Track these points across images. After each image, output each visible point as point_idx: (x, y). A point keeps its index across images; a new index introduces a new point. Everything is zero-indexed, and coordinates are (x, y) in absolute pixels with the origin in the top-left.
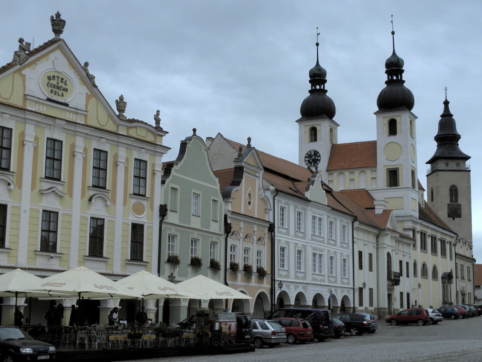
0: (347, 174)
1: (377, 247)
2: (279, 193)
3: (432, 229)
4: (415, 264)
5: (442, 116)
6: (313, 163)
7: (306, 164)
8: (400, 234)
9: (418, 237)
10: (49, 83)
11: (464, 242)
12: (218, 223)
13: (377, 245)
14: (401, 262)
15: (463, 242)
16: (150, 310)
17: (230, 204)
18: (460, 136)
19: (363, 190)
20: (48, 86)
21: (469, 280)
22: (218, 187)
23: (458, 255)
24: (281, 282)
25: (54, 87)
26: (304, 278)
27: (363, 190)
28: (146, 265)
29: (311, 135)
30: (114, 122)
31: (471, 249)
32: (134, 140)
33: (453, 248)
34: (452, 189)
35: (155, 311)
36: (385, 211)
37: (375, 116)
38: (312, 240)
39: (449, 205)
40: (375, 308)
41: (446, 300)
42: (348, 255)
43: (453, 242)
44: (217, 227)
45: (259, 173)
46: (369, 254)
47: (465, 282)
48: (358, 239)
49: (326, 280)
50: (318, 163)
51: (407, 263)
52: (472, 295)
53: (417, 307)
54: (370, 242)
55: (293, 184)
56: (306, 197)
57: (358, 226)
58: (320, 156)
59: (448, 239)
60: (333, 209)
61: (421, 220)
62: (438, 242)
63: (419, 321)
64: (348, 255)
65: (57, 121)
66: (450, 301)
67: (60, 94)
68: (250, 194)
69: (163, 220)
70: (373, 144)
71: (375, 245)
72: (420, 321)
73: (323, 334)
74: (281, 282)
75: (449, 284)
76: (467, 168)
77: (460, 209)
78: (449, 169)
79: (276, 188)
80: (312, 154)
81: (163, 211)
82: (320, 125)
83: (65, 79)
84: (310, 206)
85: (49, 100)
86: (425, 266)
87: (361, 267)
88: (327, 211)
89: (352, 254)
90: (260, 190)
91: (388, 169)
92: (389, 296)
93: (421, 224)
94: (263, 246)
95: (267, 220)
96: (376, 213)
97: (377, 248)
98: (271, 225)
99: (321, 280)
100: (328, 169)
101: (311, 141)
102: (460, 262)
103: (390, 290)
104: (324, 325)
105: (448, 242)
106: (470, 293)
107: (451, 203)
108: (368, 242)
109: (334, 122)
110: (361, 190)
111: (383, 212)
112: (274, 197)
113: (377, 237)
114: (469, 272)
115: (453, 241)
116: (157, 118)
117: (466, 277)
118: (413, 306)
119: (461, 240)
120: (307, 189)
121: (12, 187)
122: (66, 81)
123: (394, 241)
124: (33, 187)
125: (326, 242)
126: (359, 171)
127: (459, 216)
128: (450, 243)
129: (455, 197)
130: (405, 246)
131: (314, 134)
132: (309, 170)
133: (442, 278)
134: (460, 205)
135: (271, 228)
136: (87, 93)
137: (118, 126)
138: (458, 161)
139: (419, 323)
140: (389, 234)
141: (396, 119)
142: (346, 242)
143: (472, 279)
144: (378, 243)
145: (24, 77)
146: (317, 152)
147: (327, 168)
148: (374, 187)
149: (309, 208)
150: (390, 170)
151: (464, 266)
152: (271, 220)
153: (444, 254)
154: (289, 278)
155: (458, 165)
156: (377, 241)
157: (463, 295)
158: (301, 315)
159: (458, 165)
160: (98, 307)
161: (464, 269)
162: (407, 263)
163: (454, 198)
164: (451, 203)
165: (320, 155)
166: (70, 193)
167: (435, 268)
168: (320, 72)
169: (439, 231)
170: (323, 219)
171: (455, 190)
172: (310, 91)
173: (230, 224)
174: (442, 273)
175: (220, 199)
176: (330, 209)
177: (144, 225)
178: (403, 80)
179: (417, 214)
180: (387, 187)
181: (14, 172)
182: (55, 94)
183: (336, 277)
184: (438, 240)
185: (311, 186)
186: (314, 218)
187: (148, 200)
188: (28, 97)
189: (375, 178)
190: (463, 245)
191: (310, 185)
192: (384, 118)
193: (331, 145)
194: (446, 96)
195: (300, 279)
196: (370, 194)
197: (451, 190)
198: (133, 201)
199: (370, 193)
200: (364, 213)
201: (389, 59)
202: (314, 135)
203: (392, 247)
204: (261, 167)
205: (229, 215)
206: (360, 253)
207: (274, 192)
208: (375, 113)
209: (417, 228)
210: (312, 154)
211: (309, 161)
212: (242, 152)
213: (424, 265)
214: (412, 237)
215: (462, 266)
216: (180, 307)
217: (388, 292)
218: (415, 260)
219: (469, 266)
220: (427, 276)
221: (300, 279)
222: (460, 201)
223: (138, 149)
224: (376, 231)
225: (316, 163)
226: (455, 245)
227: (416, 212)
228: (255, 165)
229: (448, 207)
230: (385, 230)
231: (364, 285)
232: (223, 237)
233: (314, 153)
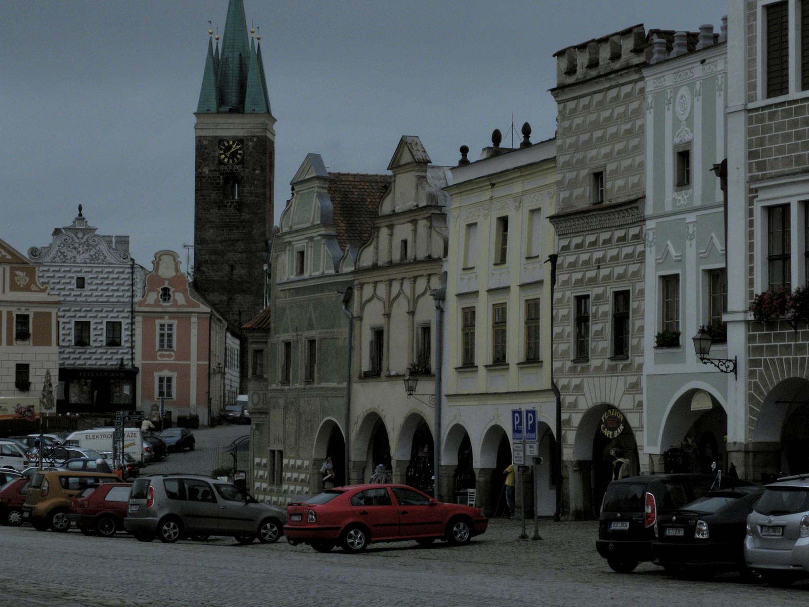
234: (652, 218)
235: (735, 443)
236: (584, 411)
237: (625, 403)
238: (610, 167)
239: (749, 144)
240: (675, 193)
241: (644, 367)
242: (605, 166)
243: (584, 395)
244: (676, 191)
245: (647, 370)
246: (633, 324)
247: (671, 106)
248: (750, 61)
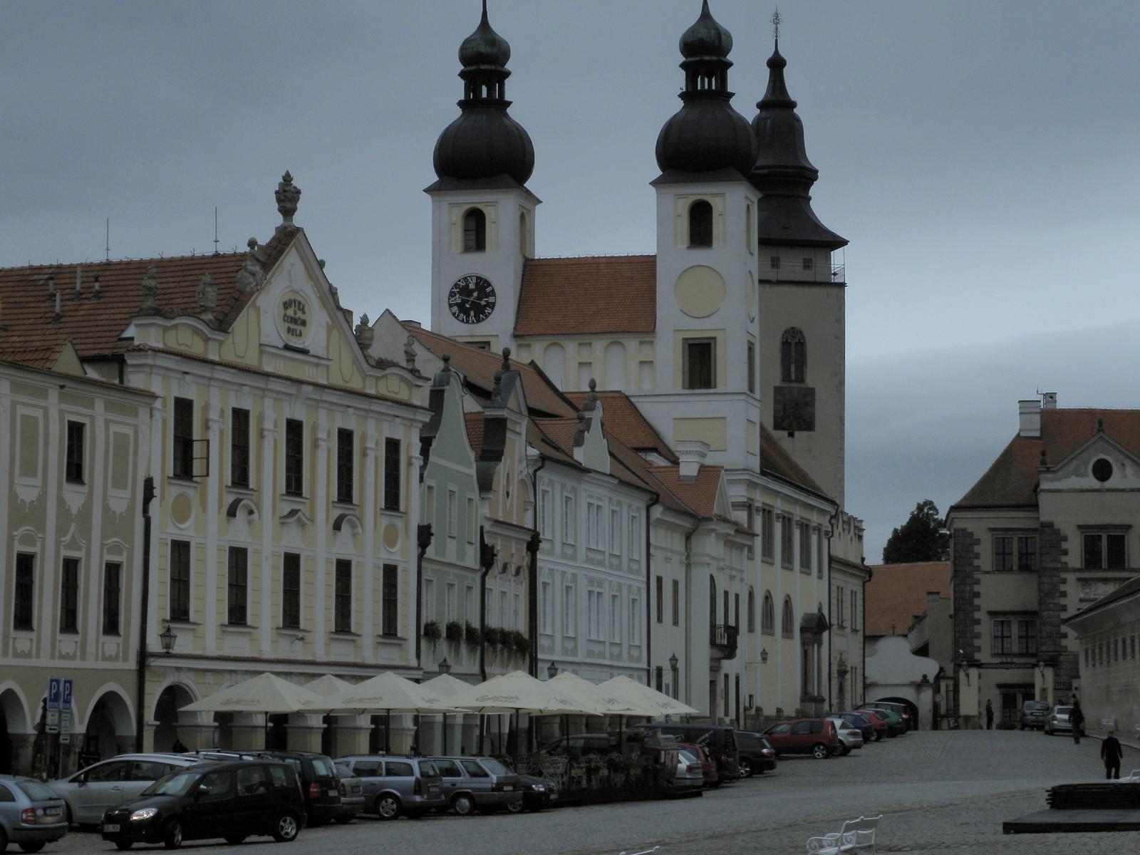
0: (571, 346)
1: (686, 562)
2: (547, 463)
3: (786, 498)
4: (751, 595)
5: (761, 106)
6: (472, 313)
7: (454, 314)
8: (735, 528)
9: (758, 521)
10: (285, 315)
11: (846, 520)
12: (474, 546)
13: (688, 557)
14: (726, 593)
15: (844, 522)
16: (409, 730)
17: (487, 504)
18: (817, 171)
19: (617, 395)
20: (284, 320)
21: (855, 631)
22: (472, 471)
23: (835, 561)
24: (553, 663)
25: (291, 322)
26: (574, 652)
27: (617, 395)
28: (353, 641)
29: (466, 230)
30: (361, 371)
31: (860, 538)
32: (390, 404)
33: (825, 542)
34: (789, 341)
35: (413, 733)
36: (703, 468)
37: (653, 190)
38: (589, 560)
39: (777, 390)
40: (731, 720)
41: (810, 689)
42: (639, 589)
43: (825, 526)
44: (472, 558)
45: (520, 424)
46: (674, 580)
47: (844, 636)
48: (656, 548)
49: (625, 655)
50: (489, 314)
51: (737, 596)
52: (860, 671)
53: (753, 712)
54: (660, 547)
55: (534, 422)
56: (576, 461)
57: (659, 516)
58: (493, 293)
59: (815, 519)
60: (622, 482)
61: (766, 478)
62: (795, 530)
63: (816, 749)
64: (639, 589)
65: (306, 388)
66: (816, 694)
67: (298, 333)
68: (508, 475)
69: (425, 553)
70: (646, 266)
71: (684, 558)
72: (819, 748)
73: (726, 773)
74: (553, 664)
75: (816, 645)
76: (835, 274)
77: (811, 403)
78: (781, 278)
79: (541, 453)
80: (472, 286)
81: (425, 535)
82: (494, 204)
83: (303, 302)
84: (585, 481)
85: (287, 348)
86: (769, 600)
87: (660, 619)
88: (610, 489)
89: (644, 586)
90: (521, 462)
91: (685, 340)
92: (713, 683)
93: (766, 489)
94: (508, 583)
95: (515, 523)
96: (681, 474)
97: (688, 566)
98: (533, 537)
99: (601, 655)
100: (517, 333)
101: (467, 249)
102: (839, 579)
103: (715, 669)
104: (729, 756)
105: (814, 529)
106: (856, 668)
107: (785, 385)
108: (672, 552)
109: (529, 194)
110: (611, 395)
111: (699, 471)
112: (535, 471)
113: (688, 537)
114: (854, 605)
115: (825, 521)
116: (409, 350)
117: (847, 624)
118: (745, 709)
119: (852, 522)
120: (579, 441)
121: (256, 516)
122: (304, 306)
123: (722, 543)
124: (274, 513)
125: (625, 565)
126: (608, 341)
127: (809, 426)
128: (819, 529)
129: (795, 366)
130: (734, 551)
131: (475, 225)
132: (534, 371)
133: (803, 630)
134: (811, 392)
135: (533, 545)
136: (327, 323)
137: (365, 376)
138: (807, 254)
139: (816, 752)
140: (713, 530)
141: (711, 202)
142: (636, 557)
143: (860, 627)
144: (690, 554)
145: (257, 309)
146: (486, 281)
147: (515, 328)
148: (647, 387)
149: (584, 486)
150: (691, 342)
151: (844, 590)
152: (530, 526)
153: (806, 564)
154: (576, 655)
155: (807, 264)
156: (686, 547)
157: (842, 673)
158: (683, 737)
159: (807, 264)
160: (285, 725)
161: (844, 597)
162: (737, 596)
163: (793, 369)
164: (785, 385)
165: (493, 291)
166: (312, 520)
167: (787, 603)
168: (495, 50)
169: (799, 500)
170: (619, 513)
171: (796, 343)
172: (461, 104)
173: (493, 547)
174: (802, 615)
175: (475, 495)
176: (616, 482)
177: (396, 566)
178: (729, 91)
179: (755, 463)
180: (684, 388)
181: (253, 490)
182: (293, 334)
183: (574, 638)
184: (795, 526)
185: (586, 433)
186: (590, 505)
187: (401, 517)
188: (268, 349)
189: (651, 362)
190: (844, 530)
191: (583, 431)
192: (679, 196)
193: (524, 259)
194: (776, 40)
195: (569, 653)
196: (635, 408)
197: (785, 344)
198: (384, 522)
199: (637, 404)
200: (650, 472)
201: (692, 30)
202: (474, 232)
203: (718, 560)
204: (525, 412)
205: (487, 527)
206: (659, 580)
207: (536, 461)
208: (654, 183)
209: (757, 501)
210: (472, 286)
211: (461, 307)
212: (501, 385)
213: (768, 598)
214: (746, 526)
215: (840, 589)
216: (454, 724)
217: (711, 676)
218: (788, 596)
219: (841, 586)
220: (791, 631)
221: (569, 653)
222: (811, 379)
223: (390, 419)
224: (687, 524)
225: (483, 313)
226: (829, 535)
227: (755, 455)
228: (515, 410)
229: (775, 396)
230: (709, 519)
231: (672, 662)
232: (478, 577)
233: (477, 284)
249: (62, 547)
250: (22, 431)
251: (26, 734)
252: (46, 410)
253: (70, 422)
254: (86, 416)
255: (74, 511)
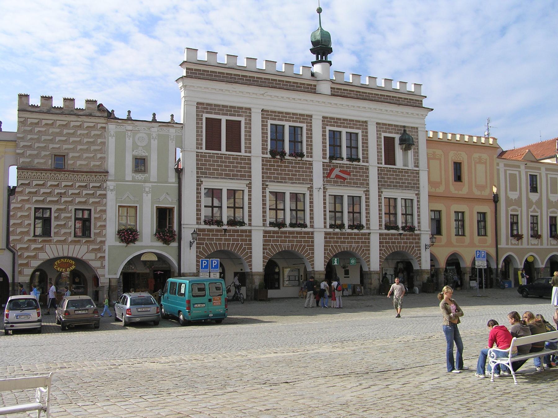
234: (111, 181)
235: (190, 273)
236: (44, 260)
237: (89, 257)
238: (71, 155)
239: (197, 164)
240: (134, 174)
241: (106, 242)
242: (68, 154)
243: (46, 252)
244: (134, 173)
245: (107, 244)
246: (95, 224)
247: (131, 139)
248: (199, 135)
249: (530, 212)
250: (509, 177)
251: (518, 268)
252: (520, 172)
253: (530, 175)
254: (538, 173)
255: (534, 201)
